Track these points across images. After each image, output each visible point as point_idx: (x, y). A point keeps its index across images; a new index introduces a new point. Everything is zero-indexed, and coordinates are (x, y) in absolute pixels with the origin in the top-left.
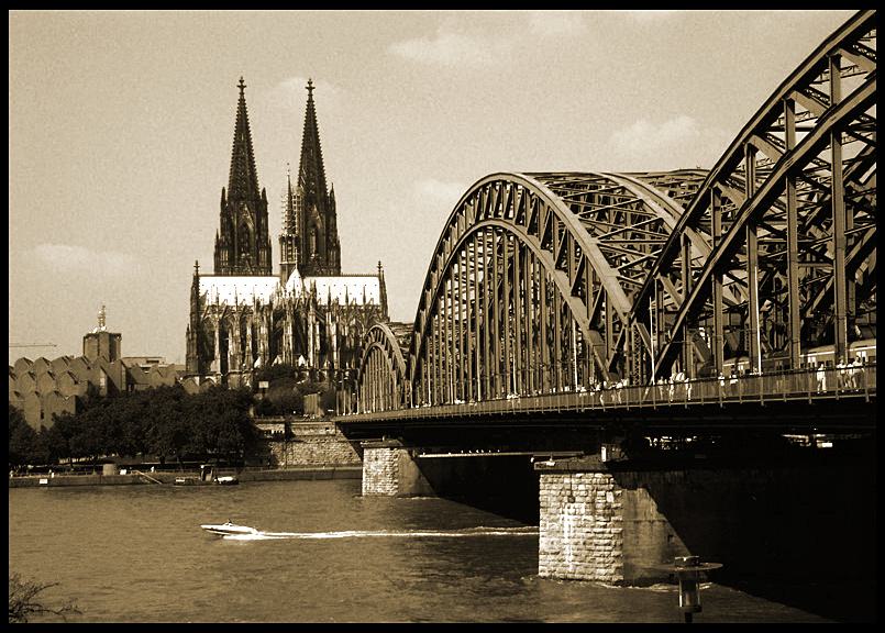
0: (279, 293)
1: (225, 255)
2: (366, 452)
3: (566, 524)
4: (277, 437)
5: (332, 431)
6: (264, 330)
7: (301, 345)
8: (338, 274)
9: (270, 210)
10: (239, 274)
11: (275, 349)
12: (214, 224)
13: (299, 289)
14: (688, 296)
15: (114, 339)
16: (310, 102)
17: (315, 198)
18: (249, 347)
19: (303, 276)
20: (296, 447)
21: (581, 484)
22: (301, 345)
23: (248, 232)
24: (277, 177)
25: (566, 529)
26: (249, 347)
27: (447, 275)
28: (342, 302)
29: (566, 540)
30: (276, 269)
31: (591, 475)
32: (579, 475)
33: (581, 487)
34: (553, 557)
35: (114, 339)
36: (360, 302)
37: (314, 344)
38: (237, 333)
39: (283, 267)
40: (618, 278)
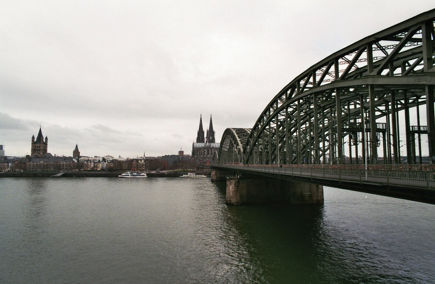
0: (205, 145)
1: (198, 140)
4: (201, 168)
5: (210, 167)
6: (203, 151)
8: (215, 143)
9: (205, 133)
10: (200, 143)
12: (196, 136)
13: (208, 145)
14: (250, 149)
15: (183, 152)
16: (211, 118)
18: (201, 154)
20: (204, 170)
22: (208, 154)
24: (206, 128)
26: (201, 154)
27: (222, 144)
28: (215, 147)
29: (231, 191)
30: (205, 142)
32: (233, 180)
34: (228, 194)
35: (183, 152)
37: (210, 153)
38: (199, 151)
39: (206, 142)
40: (242, 146)
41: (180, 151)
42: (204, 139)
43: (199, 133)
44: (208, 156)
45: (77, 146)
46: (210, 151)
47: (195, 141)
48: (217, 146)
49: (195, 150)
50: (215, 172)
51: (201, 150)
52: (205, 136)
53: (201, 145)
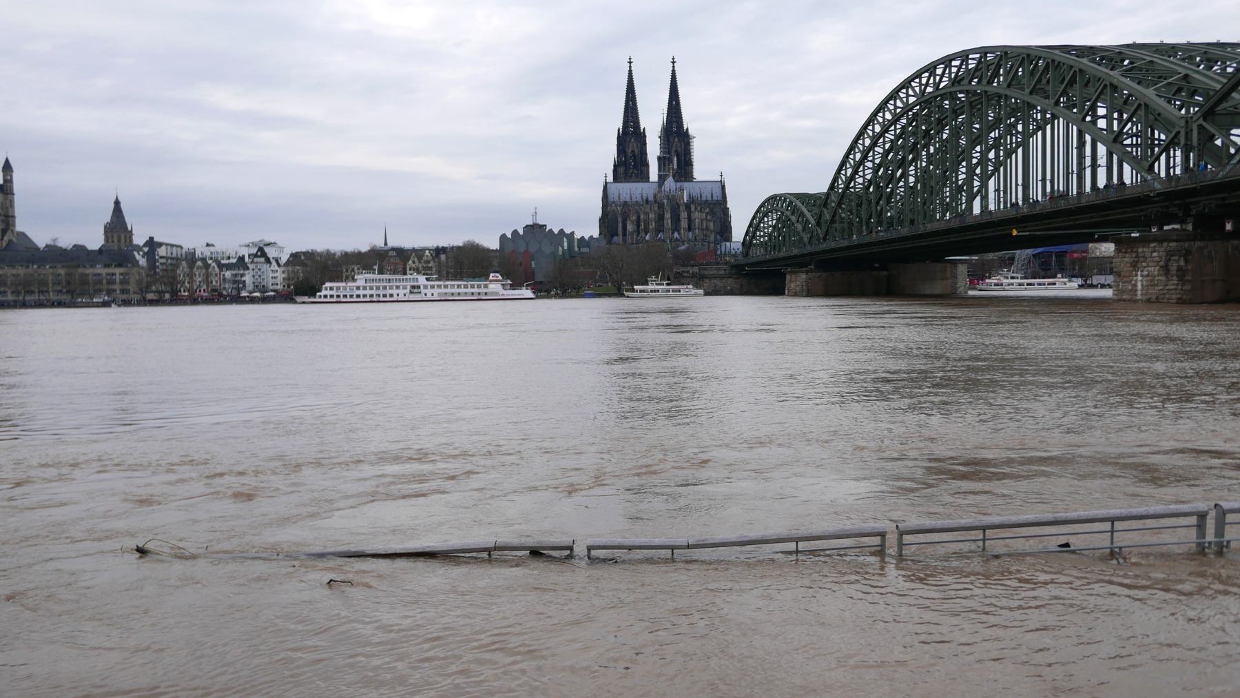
1: (621, 170)
2: (788, 277)
3: (1139, 284)
6: (652, 216)
7: (676, 226)
11: (660, 229)
17: (676, 135)
19: (676, 181)
21: (1155, 253)
23: (634, 155)
25: (1139, 287)
31: (1165, 244)
33: (1155, 254)
36: (709, 198)
37: (684, 224)
39: (660, 176)
41: (531, 223)
42: (647, 165)
43: (622, 140)
44: (676, 235)
45: (117, 203)
46: (684, 215)
47: (610, 179)
48: (706, 196)
49: (611, 217)
50: (804, 276)
51: (647, 214)
52: (653, 148)
53: (631, 191)
